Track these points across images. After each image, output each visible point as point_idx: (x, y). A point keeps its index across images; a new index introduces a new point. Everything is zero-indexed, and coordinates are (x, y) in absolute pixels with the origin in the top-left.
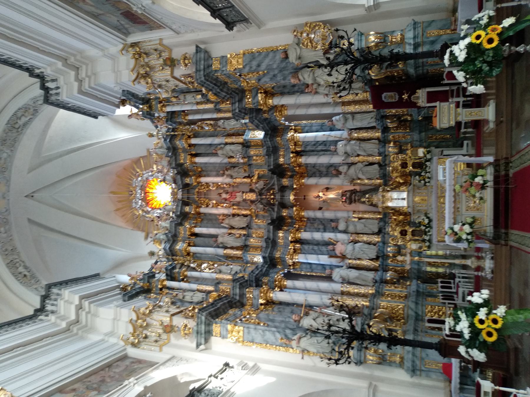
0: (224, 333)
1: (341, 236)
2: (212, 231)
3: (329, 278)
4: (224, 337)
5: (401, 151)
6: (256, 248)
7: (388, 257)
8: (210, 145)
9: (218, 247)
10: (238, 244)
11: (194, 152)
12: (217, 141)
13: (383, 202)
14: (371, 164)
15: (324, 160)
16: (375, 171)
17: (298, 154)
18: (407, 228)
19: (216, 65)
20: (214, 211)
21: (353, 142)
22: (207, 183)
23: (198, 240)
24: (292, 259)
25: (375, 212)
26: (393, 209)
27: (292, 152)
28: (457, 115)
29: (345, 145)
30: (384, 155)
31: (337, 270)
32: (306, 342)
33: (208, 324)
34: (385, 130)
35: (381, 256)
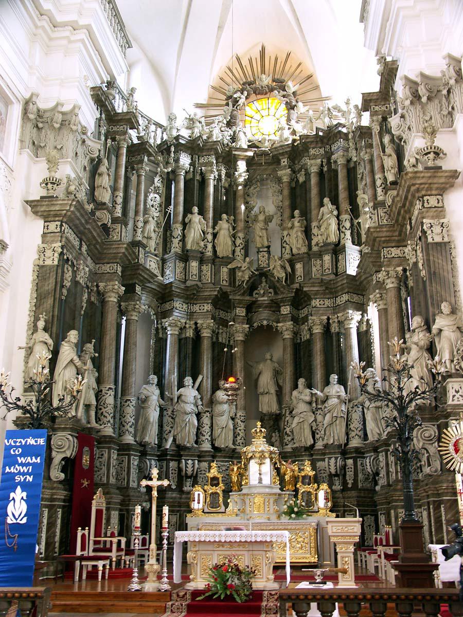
4: (44, 235)
10: (189, 247)
16: (303, 441)
24: (169, 325)
26: (246, 468)
27: (328, 319)
31: (157, 392)
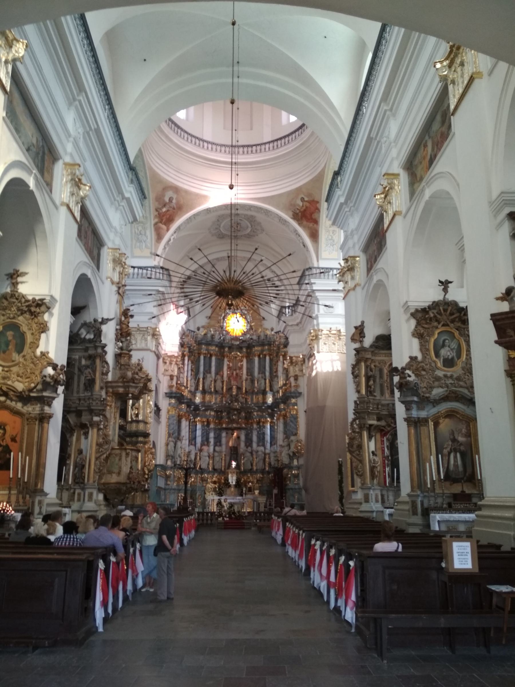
0: (172, 405)
1: (211, 448)
2: (213, 369)
3: (190, 443)
4: (170, 404)
5: (258, 481)
6: (204, 398)
7: (202, 475)
8: (265, 368)
9: (204, 374)
10: (206, 387)
11: (261, 356)
12: (267, 374)
13: (231, 472)
14: (252, 465)
15: (255, 438)
17: (258, 423)
18: (218, 484)
19: (293, 401)
20: (225, 368)
21: (263, 455)
22: (242, 361)
23: (207, 360)
25: (225, 466)
27: (259, 420)
28: (262, 503)
29: (262, 451)
30: (256, 472)
31: (194, 447)
32: (172, 444)
33: (175, 397)
34: (269, 473)
35: (202, 471)
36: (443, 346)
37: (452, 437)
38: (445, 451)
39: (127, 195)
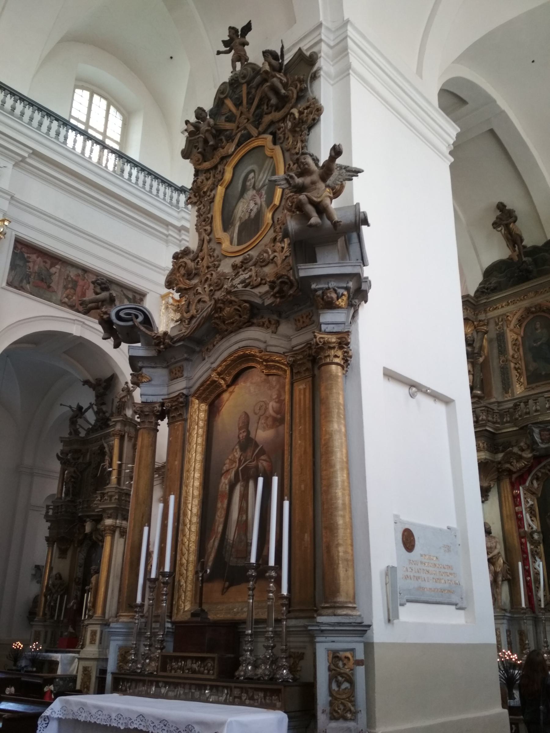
36: (244, 189)
37: (243, 435)
38: (224, 483)
39: (178, 224)
